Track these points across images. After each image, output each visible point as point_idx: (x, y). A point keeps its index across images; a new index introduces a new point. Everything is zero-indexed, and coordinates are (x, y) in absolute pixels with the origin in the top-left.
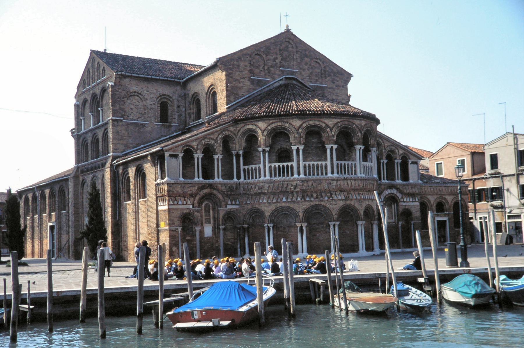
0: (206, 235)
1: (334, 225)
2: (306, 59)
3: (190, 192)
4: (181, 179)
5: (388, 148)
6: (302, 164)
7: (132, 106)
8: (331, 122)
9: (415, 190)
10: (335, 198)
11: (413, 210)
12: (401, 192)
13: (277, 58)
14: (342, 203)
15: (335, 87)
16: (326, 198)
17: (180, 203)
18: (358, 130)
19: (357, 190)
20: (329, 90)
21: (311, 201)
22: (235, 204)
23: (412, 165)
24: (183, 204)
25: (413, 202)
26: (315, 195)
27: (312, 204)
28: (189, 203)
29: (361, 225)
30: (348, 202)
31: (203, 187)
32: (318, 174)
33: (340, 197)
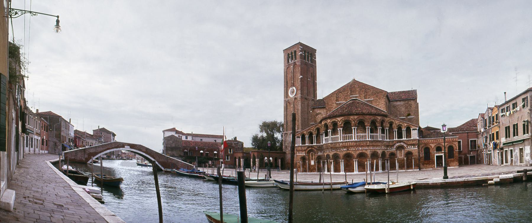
0: (312, 164)
1: (342, 161)
2: (363, 90)
3: (304, 149)
4: (301, 145)
5: (398, 124)
6: (331, 137)
7: (318, 118)
8: (339, 119)
9: (414, 142)
10: (342, 150)
11: (413, 152)
12: (406, 144)
13: (348, 92)
14: (345, 152)
15: (378, 99)
16: (339, 150)
17: (301, 153)
18: (352, 120)
19: (352, 146)
20: (375, 101)
21: (334, 152)
22: (322, 153)
23: (413, 131)
24: (302, 153)
25: (413, 148)
26: (335, 149)
27: (334, 153)
28: (304, 153)
29: (356, 161)
30: (348, 152)
31: (309, 147)
32: (348, 139)
33: (344, 150)
